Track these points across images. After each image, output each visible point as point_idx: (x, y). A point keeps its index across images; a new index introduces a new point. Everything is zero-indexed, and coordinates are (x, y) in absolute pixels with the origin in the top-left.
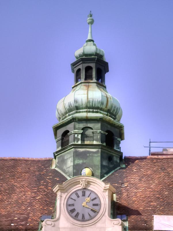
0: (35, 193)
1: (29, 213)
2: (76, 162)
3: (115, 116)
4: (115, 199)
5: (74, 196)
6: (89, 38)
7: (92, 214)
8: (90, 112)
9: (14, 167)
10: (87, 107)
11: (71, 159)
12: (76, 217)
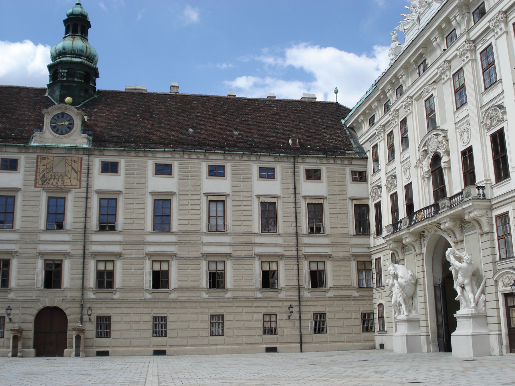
0: (31, 113)
1: (25, 127)
2: (62, 93)
3: (92, 61)
4: (86, 120)
5: (56, 118)
7: (68, 130)
8: (73, 57)
10: (71, 54)
11: (59, 90)
12: (56, 132)
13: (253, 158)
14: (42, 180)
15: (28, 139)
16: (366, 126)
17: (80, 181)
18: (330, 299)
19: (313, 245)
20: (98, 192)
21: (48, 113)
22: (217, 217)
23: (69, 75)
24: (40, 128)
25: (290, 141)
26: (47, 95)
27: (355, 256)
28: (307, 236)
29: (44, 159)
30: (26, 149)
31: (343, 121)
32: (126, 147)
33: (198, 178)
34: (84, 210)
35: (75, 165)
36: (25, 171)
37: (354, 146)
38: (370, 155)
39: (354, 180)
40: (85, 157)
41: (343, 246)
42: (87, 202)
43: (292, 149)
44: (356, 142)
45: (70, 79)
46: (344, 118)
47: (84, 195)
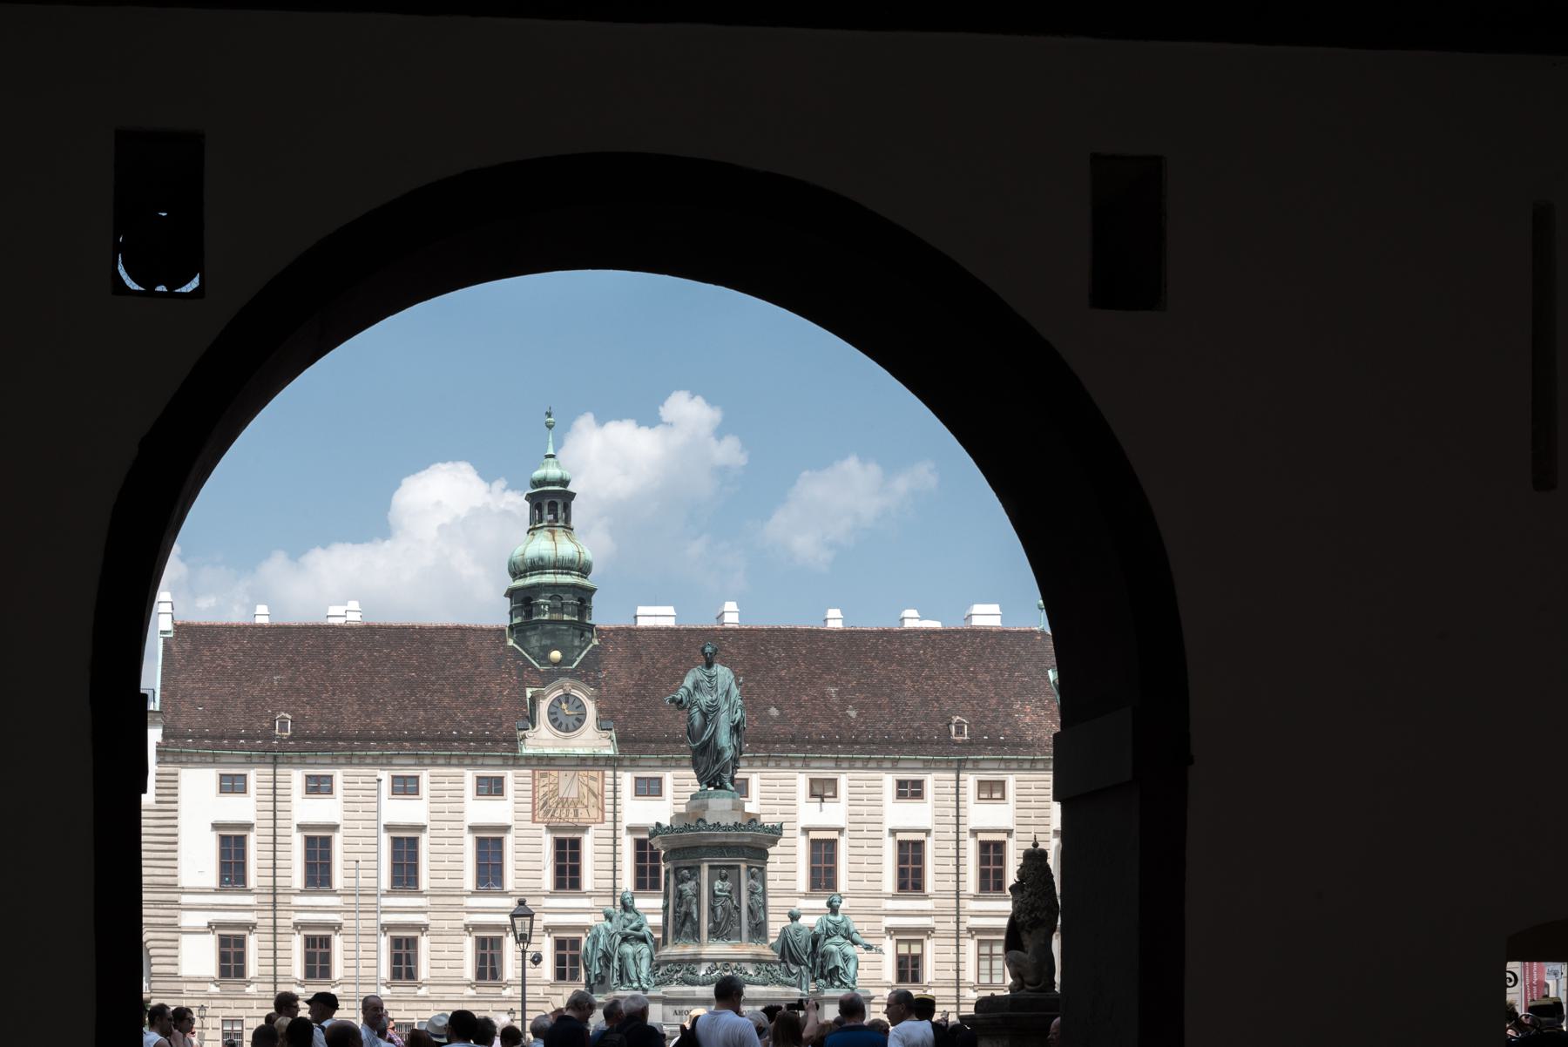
9: (463, 641)
12: (559, 728)
13: (888, 764)
15: (513, 742)
17: (603, 810)
21: (544, 697)
24: (532, 720)
26: (511, 642)
28: (976, 898)
29: (543, 776)
30: (517, 761)
33: (791, 802)
34: (611, 857)
35: (593, 784)
40: (609, 773)
42: (615, 845)
47: (611, 834)
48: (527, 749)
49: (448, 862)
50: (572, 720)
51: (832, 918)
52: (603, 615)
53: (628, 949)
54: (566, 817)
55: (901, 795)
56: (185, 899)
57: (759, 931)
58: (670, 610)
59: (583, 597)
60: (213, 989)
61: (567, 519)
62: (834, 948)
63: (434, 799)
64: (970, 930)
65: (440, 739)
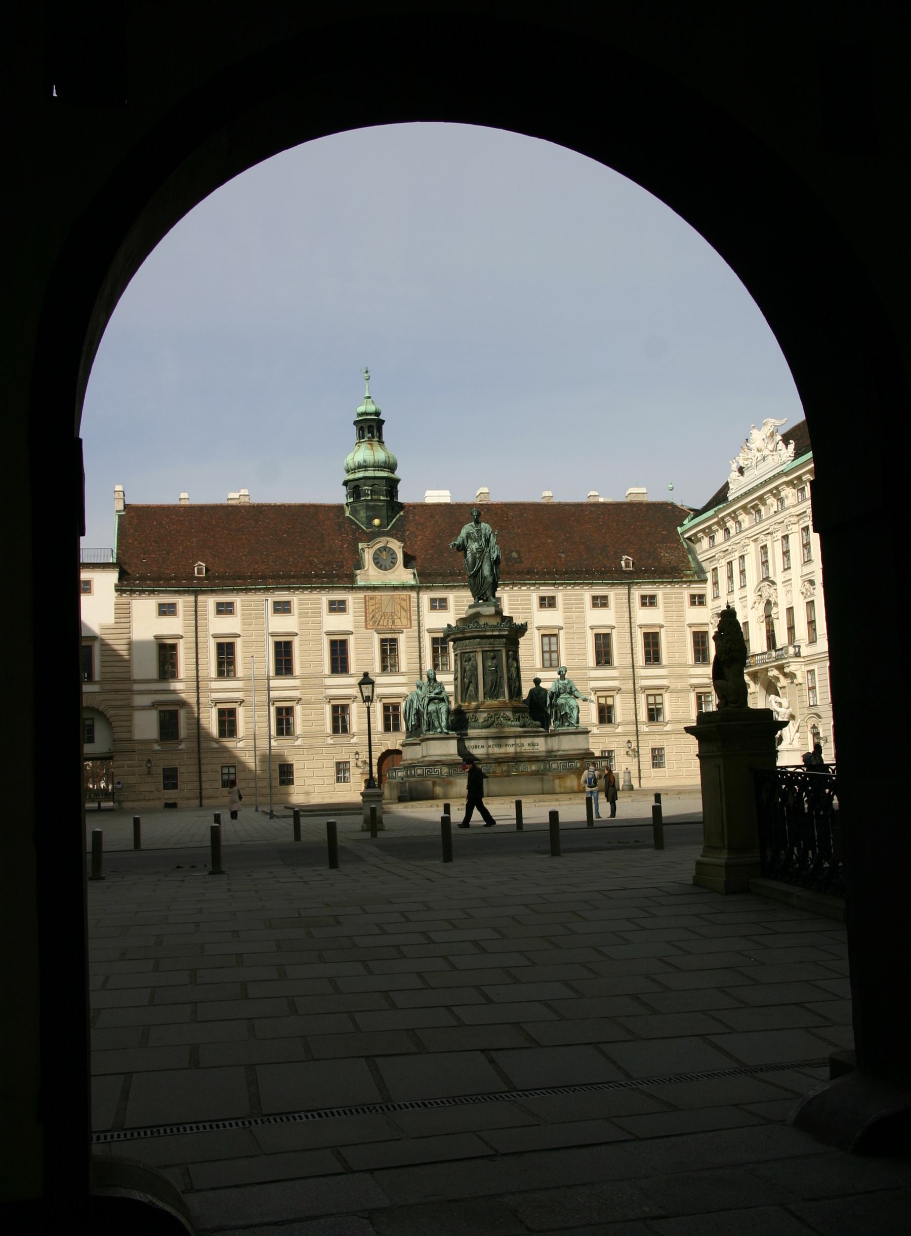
6: (367, 395)
10: (373, 466)
12: (380, 568)
14: (371, 620)
15: (352, 578)
16: (705, 542)
17: (410, 620)
18: (668, 733)
19: (649, 676)
20: (430, 631)
22: (550, 652)
23: (373, 492)
25: (623, 563)
26: (347, 514)
27: (694, 686)
29: (372, 598)
30: (354, 589)
31: (680, 530)
32: (454, 581)
36: (355, 612)
37: (693, 565)
38: (709, 576)
39: (693, 603)
40: (414, 594)
41: (680, 677)
43: (625, 572)
44: (695, 559)
45: (375, 497)
46: (682, 525)
48: (360, 582)
49: (311, 657)
50: (388, 563)
51: (561, 682)
52: (403, 497)
53: (432, 707)
54: (385, 623)
55: (595, 605)
56: (136, 687)
57: (516, 691)
58: (447, 493)
59: (392, 485)
60: (157, 747)
61: (380, 436)
62: (563, 701)
63: (301, 615)
64: (642, 688)
65: (305, 576)
